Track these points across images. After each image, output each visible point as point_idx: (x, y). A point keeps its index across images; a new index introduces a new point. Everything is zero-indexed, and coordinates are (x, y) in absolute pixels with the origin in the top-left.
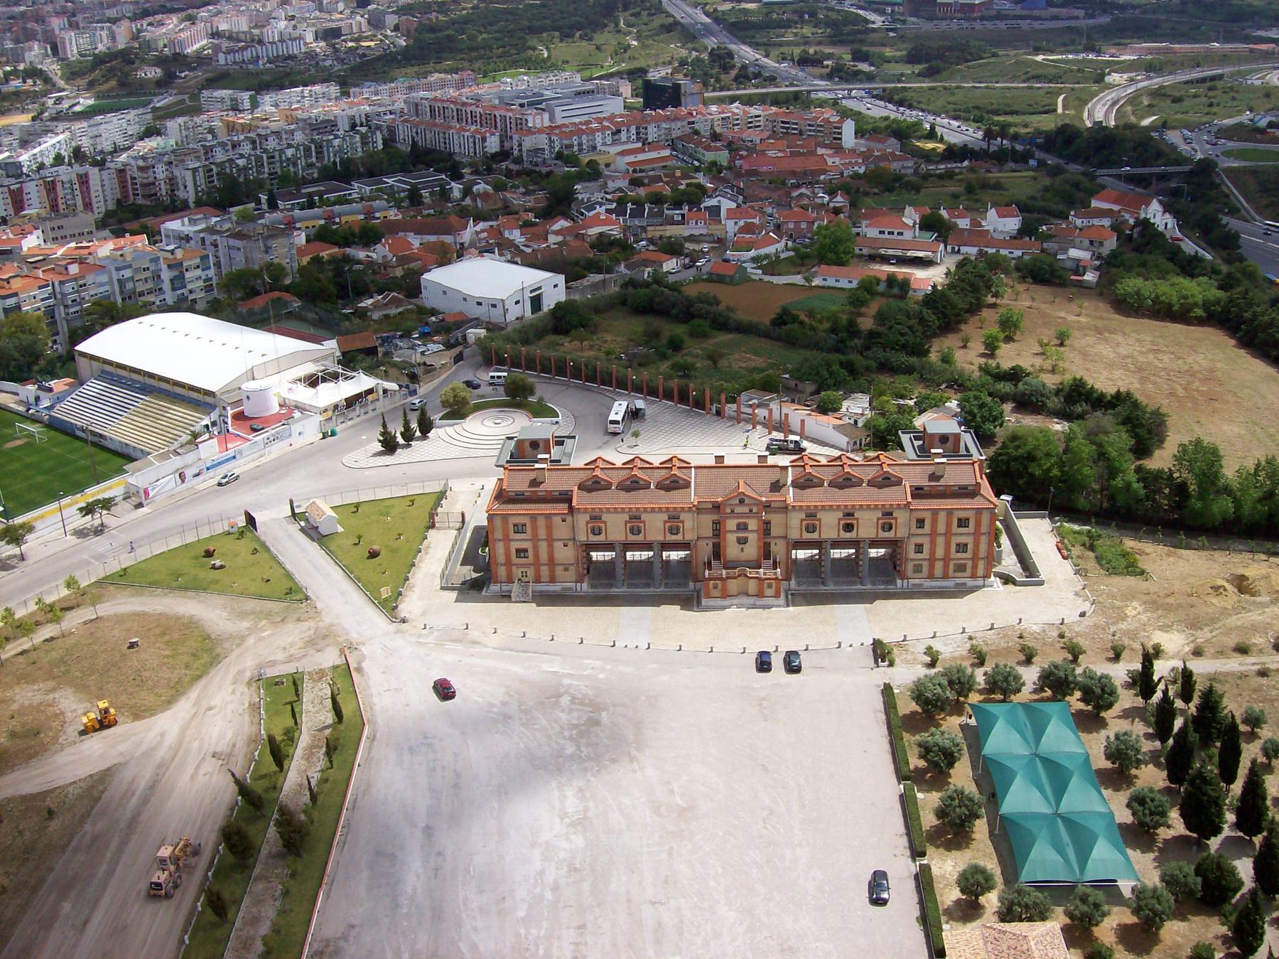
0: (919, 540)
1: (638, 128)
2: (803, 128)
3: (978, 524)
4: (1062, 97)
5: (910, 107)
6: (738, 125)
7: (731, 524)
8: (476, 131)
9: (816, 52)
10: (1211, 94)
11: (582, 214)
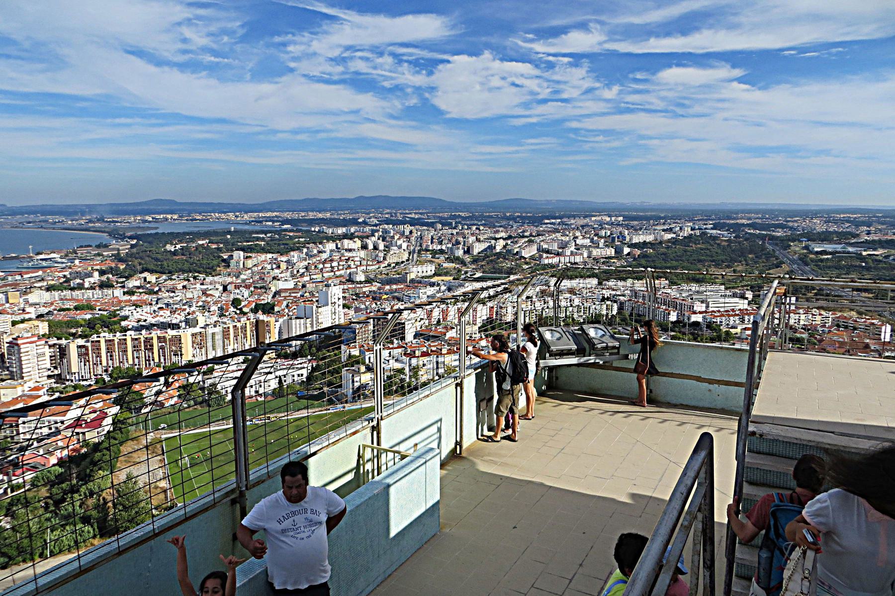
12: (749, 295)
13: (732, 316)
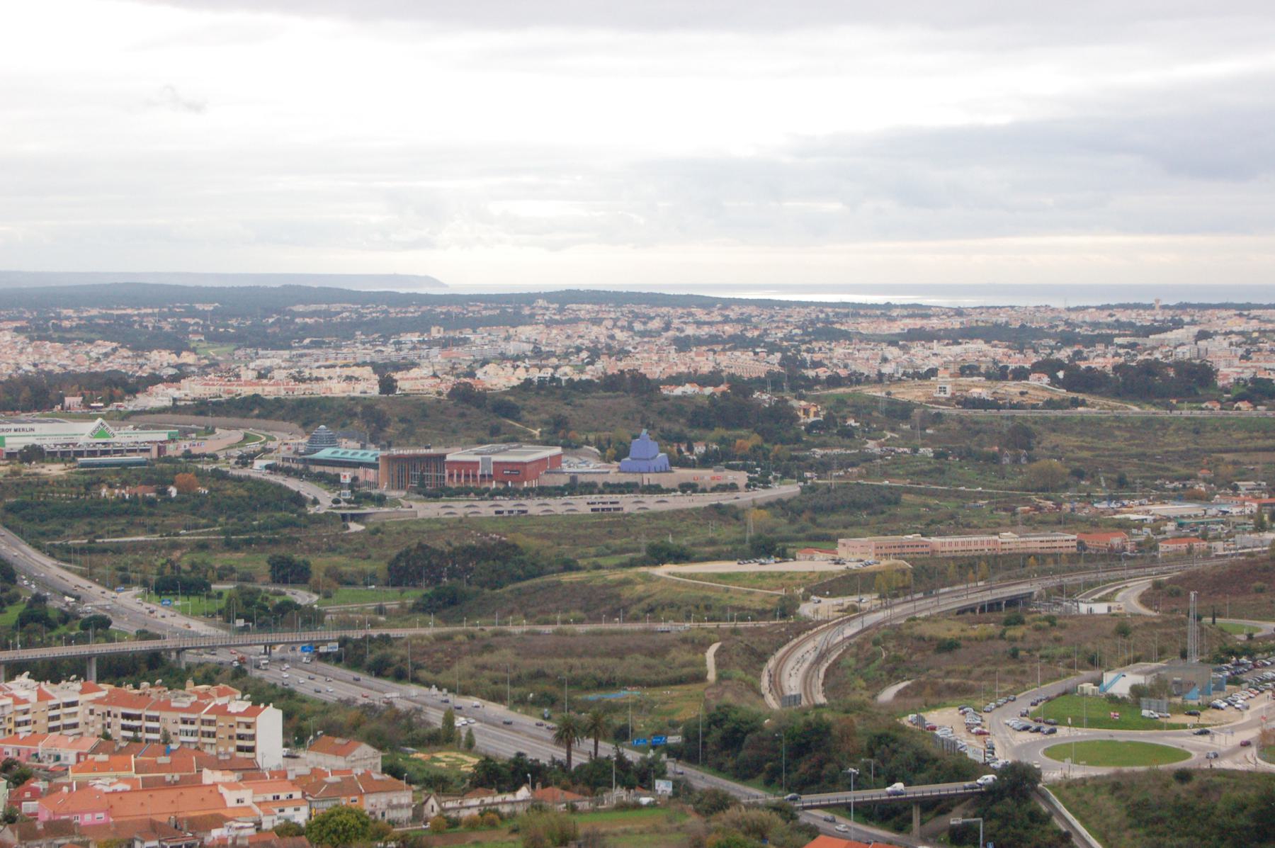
2: (172, 728)
4: (714, 648)
5: (400, 676)
6: (26, 723)
9: (194, 566)
10: (1011, 632)
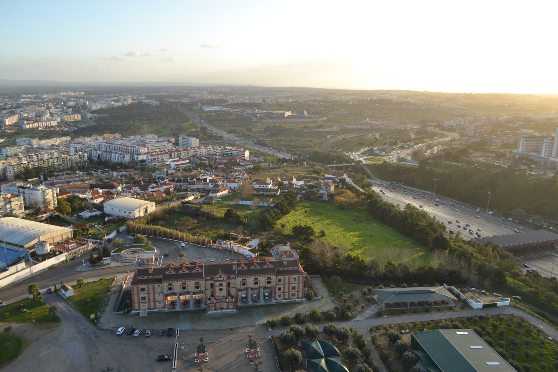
0: (280, 286)
1: (177, 153)
3: (299, 280)
7: (217, 284)
8: (121, 154)
11: (160, 182)
12: (173, 140)
13: (164, 154)
